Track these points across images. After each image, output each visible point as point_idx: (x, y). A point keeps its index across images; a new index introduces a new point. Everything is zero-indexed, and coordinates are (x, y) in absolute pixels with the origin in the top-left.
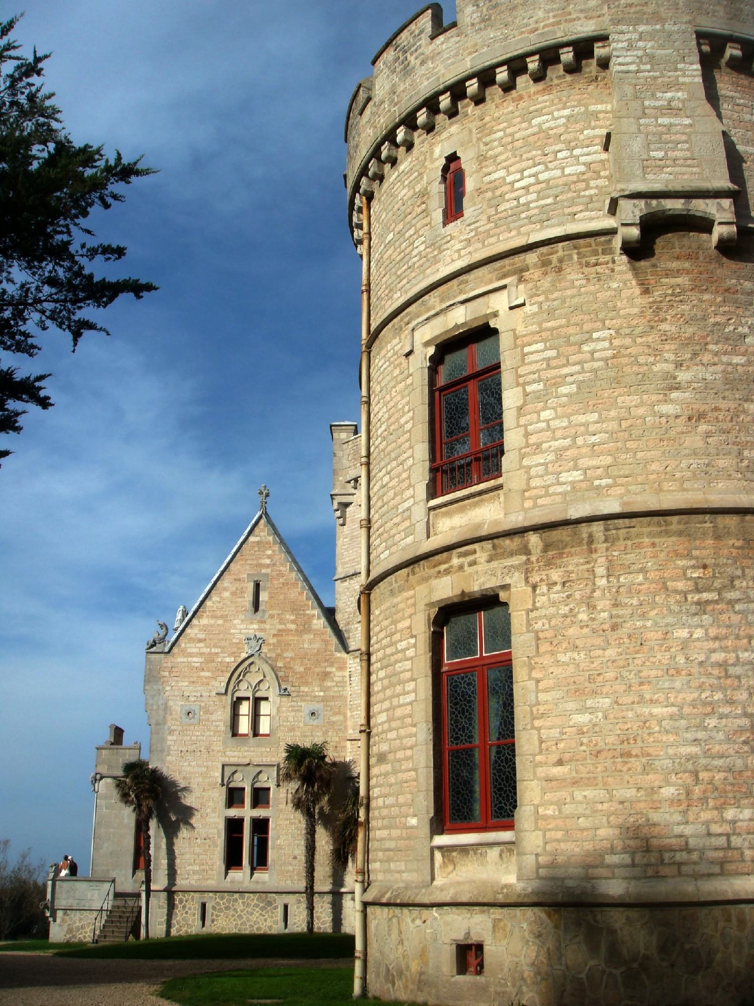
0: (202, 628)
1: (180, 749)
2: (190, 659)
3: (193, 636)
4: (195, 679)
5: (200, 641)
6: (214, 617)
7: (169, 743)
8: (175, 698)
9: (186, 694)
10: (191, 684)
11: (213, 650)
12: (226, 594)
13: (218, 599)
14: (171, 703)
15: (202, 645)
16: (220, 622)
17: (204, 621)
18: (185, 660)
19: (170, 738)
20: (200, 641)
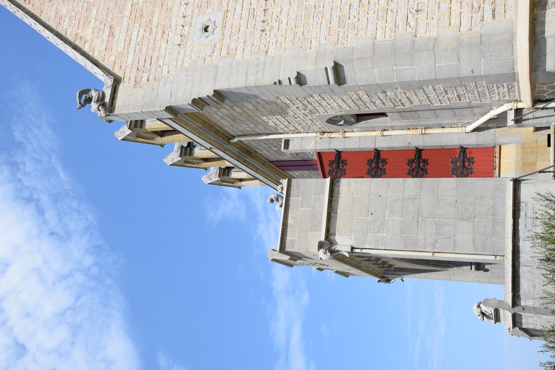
0: (95, 35)
1: (258, 33)
2: (133, 45)
3: (103, 47)
4: (160, 32)
5: (111, 34)
6: (87, 21)
7: (247, 56)
8: (180, 57)
9: (178, 40)
10: (166, 35)
11: (127, 13)
12: (63, 11)
13: (67, 20)
14: (186, 65)
15: (117, 31)
16: (94, 12)
17: (88, 34)
18: (131, 51)
19: (239, 56)
20: (111, 34)
